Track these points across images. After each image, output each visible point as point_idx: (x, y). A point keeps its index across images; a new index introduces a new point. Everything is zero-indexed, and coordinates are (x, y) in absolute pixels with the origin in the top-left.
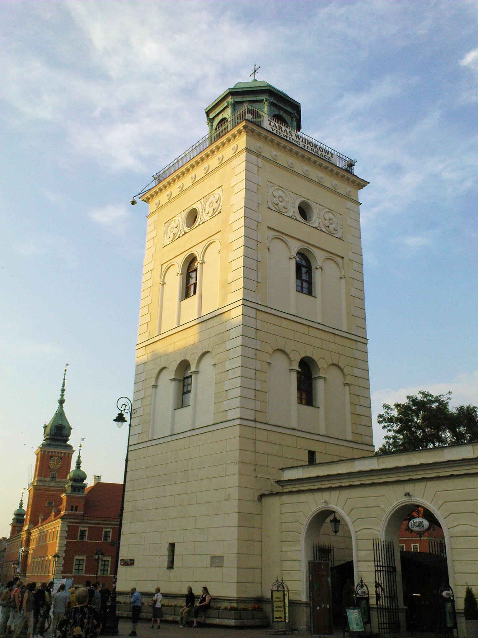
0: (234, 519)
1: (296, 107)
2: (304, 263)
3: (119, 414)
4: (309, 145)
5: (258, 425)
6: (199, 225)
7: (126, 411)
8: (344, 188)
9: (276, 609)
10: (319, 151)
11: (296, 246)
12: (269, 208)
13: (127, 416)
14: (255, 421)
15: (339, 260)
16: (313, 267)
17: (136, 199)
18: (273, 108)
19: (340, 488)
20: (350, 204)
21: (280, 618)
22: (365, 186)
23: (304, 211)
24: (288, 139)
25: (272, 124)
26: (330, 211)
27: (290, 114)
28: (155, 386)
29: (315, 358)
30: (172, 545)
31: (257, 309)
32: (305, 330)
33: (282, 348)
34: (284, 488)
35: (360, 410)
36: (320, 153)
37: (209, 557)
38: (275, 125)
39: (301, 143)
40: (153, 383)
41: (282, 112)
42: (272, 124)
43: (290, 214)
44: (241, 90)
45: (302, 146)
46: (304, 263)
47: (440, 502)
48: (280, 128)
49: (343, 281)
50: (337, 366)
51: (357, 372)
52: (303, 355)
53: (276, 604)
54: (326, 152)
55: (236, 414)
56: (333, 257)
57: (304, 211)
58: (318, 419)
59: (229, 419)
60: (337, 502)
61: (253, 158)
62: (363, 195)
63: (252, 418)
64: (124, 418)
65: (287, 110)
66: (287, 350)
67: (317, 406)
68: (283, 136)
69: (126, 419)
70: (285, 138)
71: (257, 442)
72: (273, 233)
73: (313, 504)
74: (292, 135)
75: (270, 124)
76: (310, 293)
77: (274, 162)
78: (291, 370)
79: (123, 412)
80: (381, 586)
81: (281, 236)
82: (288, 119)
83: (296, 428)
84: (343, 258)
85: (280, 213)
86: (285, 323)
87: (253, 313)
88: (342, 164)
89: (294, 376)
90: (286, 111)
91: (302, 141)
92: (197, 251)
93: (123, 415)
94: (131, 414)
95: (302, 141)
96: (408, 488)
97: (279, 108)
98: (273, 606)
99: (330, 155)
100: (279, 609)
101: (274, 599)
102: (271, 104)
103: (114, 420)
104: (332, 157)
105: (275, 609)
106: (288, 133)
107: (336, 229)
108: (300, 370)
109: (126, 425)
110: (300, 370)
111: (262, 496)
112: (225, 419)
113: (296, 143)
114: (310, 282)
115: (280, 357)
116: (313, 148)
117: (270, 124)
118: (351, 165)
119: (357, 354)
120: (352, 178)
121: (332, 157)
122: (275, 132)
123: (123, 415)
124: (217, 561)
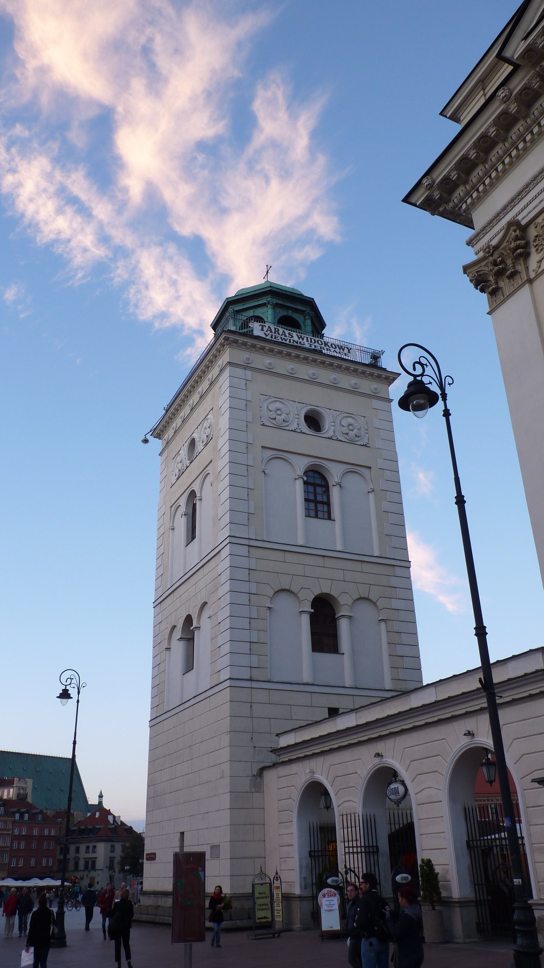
0: (225, 801)
1: (310, 303)
2: (318, 481)
3: (63, 690)
4: (316, 344)
5: (255, 685)
6: (197, 456)
7: (72, 685)
8: (367, 385)
9: (259, 907)
10: (331, 349)
11: (301, 465)
12: (263, 425)
13: (73, 692)
14: (251, 680)
16: (330, 485)
18: (278, 310)
19: (323, 753)
20: (376, 403)
21: (265, 918)
22: (394, 379)
23: (313, 421)
24: (287, 342)
26: (350, 415)
27: (302, 312)
28: (168, 649)
31: (249, 546)
32: (319, 561)
33: (287, 588)
34: (284, 757)
35: (401, 650)
37: (209, 846)
39: (306, 343)
40: (166, 646)
41: (290, 312)
43: (294, 427)
44: (240, 297)
46: (318, 481)
47: (408, 762)
49: (371, 495)
50: (367, 599)
51: (395, 604)
52: (317, 592)
55: (226, 674)
56: (354, 468)
57: (313, 421)
58: (341, 668)
59: (221, 681)
60: (322, 771)
61: (240, 372)
63: (248, 677)
64: (70, 694)
66: (294, 589)
67: (342, 652)
68: (280, 340)
69: (71, 696)
70: (284, 341)
72: (269, 454)
73: (299, 775)
74: (292, 337)
75: (262, 330)
77: (269, 372)
79: (68, 688)
80: (354, 872)
81: (280, 454)
83: (311, 682)
84: (370, 468)
85: (279, 428)
86: (290, 557)
87: (244, 550)
91: (307, 341)
92: (196, 487)
93: (68, 690)
94: (78, 689)
95: (307, 341)
96: (379, 747)
99: (346, 351)
100: (264, 907)
101: (257, 895)
102: (276, 306)
103: (57, 697)
104: (349, 352)
105: (269, 906)
106: (287, 335)
107: (358, 435)
108: (313, 611)
109: (72, 702)
110: (313, 611)
111: (262, 770)
112: (219, 682)
113: (299, 345)
115: (284, 598)
116: (323, 346)
117: (262, 330)
118: (376, 357)
119: (394, 582)
121: (349, 352)
122: (269, 337)
123: (68, 690)
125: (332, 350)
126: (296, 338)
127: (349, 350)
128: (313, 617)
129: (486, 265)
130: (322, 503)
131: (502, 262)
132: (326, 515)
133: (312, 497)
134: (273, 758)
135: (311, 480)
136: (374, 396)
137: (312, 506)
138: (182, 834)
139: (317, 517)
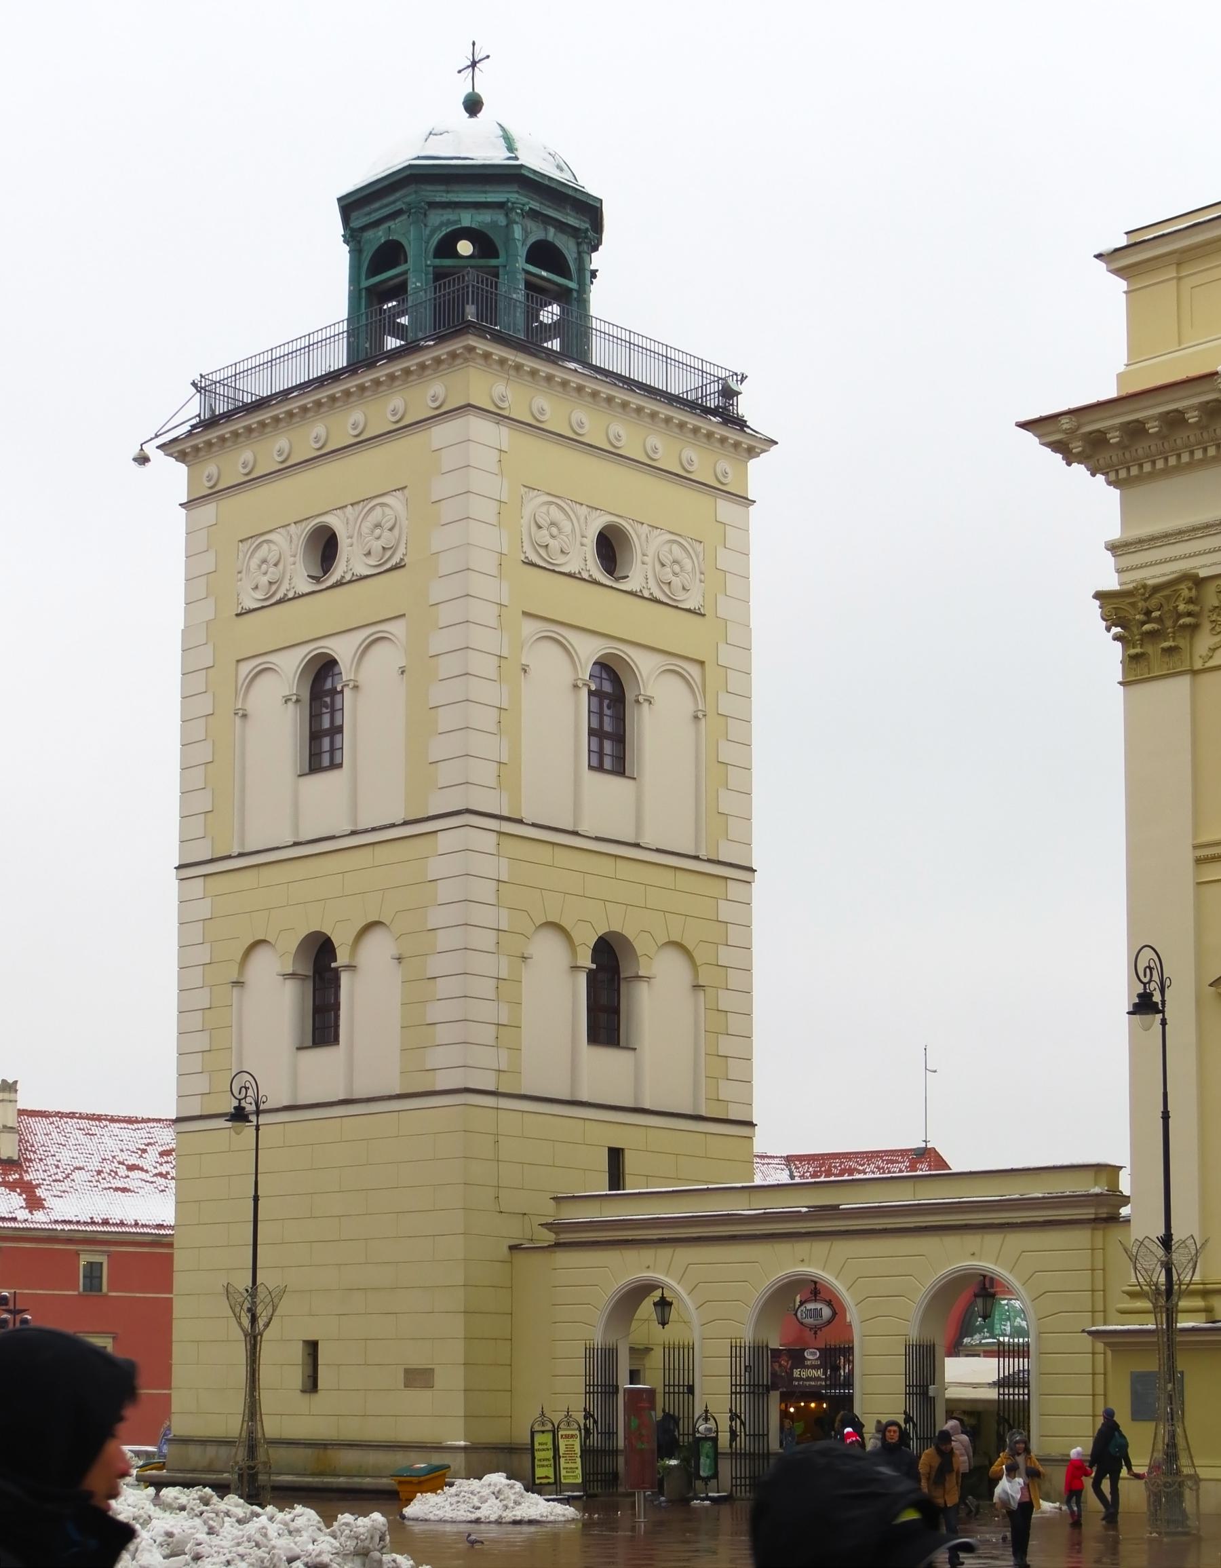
11: (589, 650)
15: (694, 670)
17: (150, 450)
20: (726, 509)
23: (610, 548)
29: (629, 933)
30: (312, 1347)
31: (500, 833)
53: (538, 1455)
57: (610, 548)
62: (759, 474)
71: (500, 1139)
76: (620, 768)
78: (575, 968)
89: (582, 979)
90: (562, 227)
97: (547, 220)
98: (533, 1458)
108: (594, 966)
110: (594, 966)
114: (619, 738)
118: (729, 393)
120: (733, 435)
124: (418, 1378)
128: (592, 977)
129: (1133, 605)
131: (1160, 620)
134: (549, 1237)
138: (312, 1347)
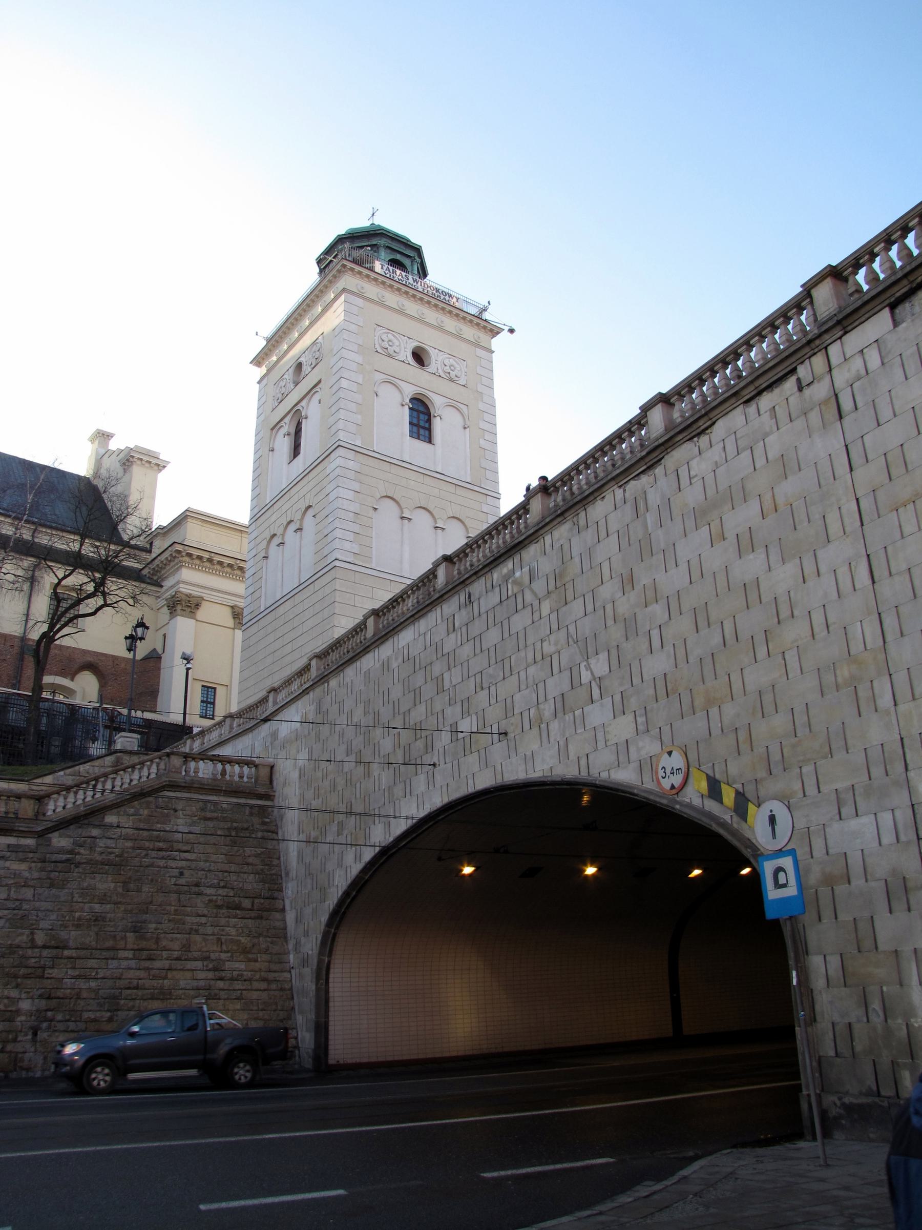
1: (418, 250)
2: (422, 409)
20: (480, 352)
22: (498, 333)
25: (385, 268)
36: (442, 297)
38: (388, 269)
42: (385, 268)
45: (421, 290)
46: (422, 409)
48: (394, 272)
54: (450, 296)
65: (405, 255)
82: (407, 262)
88: (473, 311)
99: (455, 300)
125: (442, 297)
126: (411, 281)
127: (458, 299)
130: (424, 428)
132: (427, 440)
133: (415, 421)
135: (416, 407)
136: (477, 345)
137: (415, 429)
139: (418, 438)
